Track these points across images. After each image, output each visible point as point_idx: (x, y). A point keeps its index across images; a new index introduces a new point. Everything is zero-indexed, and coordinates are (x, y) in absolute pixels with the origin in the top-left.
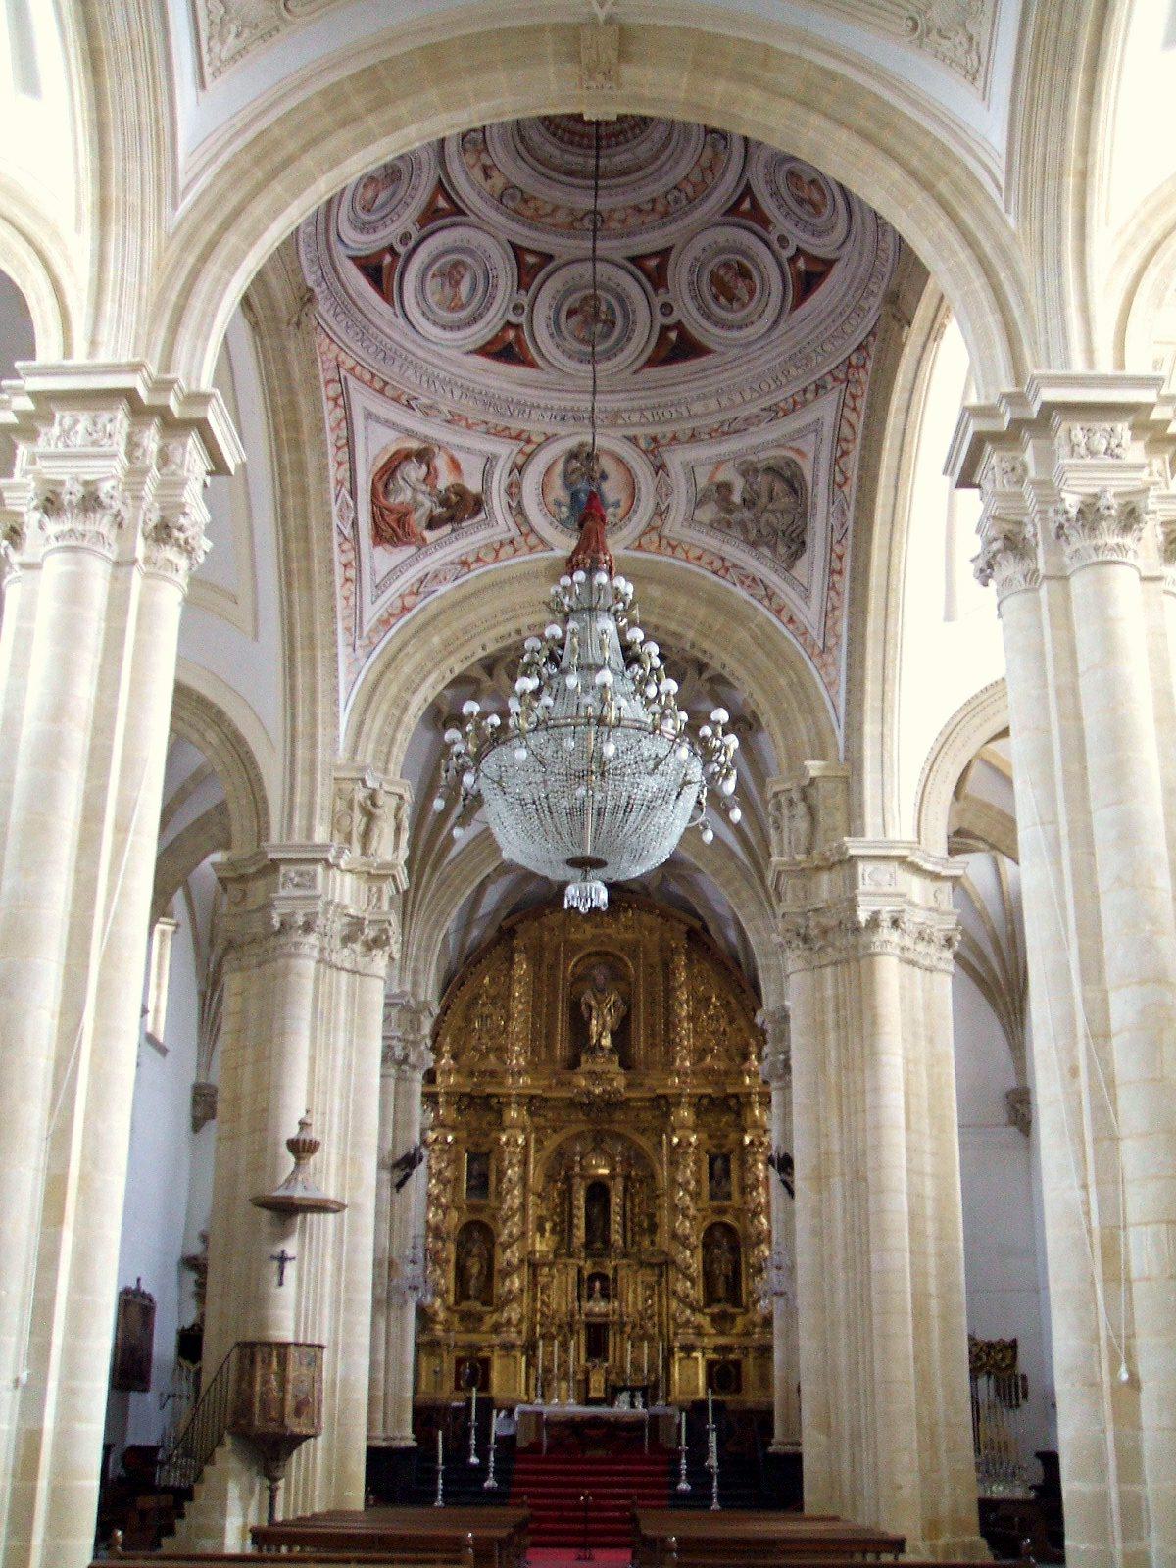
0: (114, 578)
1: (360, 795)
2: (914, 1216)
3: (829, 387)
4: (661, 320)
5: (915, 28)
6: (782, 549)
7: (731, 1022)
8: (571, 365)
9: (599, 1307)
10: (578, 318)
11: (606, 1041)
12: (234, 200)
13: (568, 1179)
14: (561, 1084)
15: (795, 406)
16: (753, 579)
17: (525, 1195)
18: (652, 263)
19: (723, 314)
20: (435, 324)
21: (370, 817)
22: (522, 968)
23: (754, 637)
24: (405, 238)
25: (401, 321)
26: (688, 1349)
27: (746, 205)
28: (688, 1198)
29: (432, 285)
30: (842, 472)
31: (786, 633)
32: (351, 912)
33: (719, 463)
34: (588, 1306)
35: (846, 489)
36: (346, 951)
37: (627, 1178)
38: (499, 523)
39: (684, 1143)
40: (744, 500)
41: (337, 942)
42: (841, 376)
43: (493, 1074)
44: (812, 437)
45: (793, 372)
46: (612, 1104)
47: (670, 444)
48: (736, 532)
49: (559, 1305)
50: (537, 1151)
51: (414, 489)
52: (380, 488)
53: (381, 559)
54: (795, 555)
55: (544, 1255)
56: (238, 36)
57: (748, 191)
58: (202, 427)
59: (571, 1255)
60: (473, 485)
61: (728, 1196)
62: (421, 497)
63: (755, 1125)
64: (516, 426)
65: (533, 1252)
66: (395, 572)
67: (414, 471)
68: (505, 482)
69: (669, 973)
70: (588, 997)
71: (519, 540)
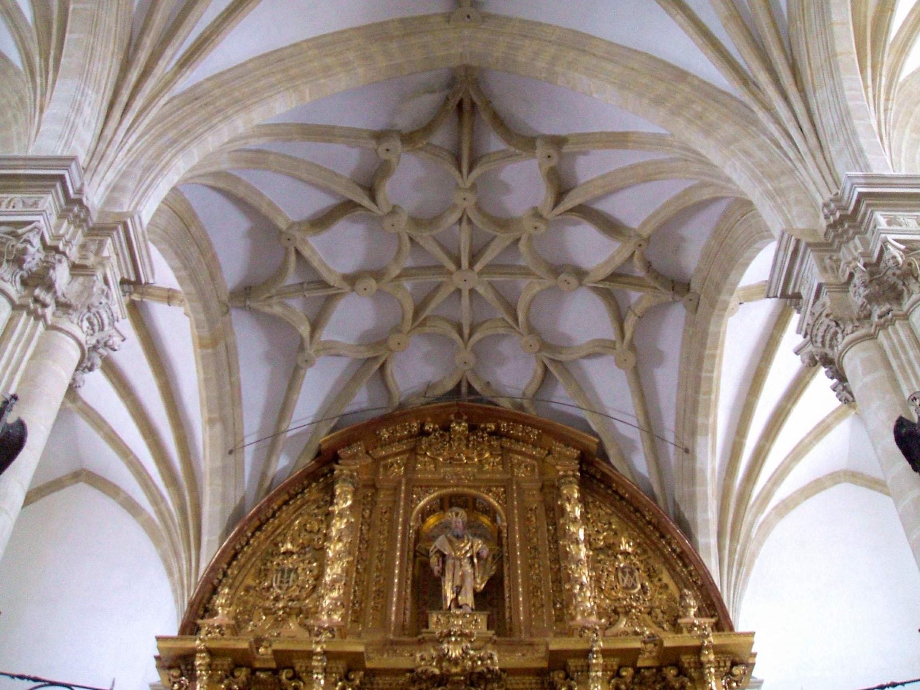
7: (651, 574)
11: (467, 599)
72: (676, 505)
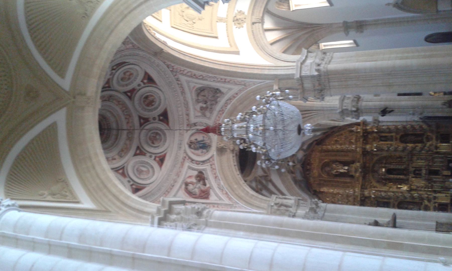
0: (211, 226)
1: (276, 207)
2: (402, 58)
3: (178, 77)
4: (157, 121)
5: (84, 17)
6: (218, 95)
7: (342, 135)
8: (167, 144)
9: (424, 172)
10: (155, 142)
11: (346, 168)
12: (111, 197)
13: (386, 179)
14: (358, 180)
15: (182, 87)
16: (226, 103)
17: (390, 192)
18: (142, 121)
19: (157, 103)
20: (152, 177)
21: (282, 205)
22: (324, 189)
23: (241, 104)
24: (129, 182)
25: (151, 185)
26: (437, 148)
27: (129, 94)
28: (392, 147)
29: (142, 177)
30: (200, 76)
31: (240, 95)
32: (308, 210)
33: (195, 109)
34: (423, 175)
35: (204, 76)
36: (319, 213)
37: (385, 164)
38: (206, 167)
39: (376, 147)
40: (205, 104)
41: (316, 215)
42: (175, 73)
43: (354, 199)
44: (190, 84)
45: (173, 87)
46: (364, 167)
47: (189, 121)
48: (213, 107)
49: (422, 183)
50: (377, 188)
51: (195, 188)
52: (194, 196)
53: (213, 198)
54: (220, 91)
55: (408, 188)
56: (66, 192)
57: (125, 93)
58: (171, 203)
59: (408, 180)
60: (196, 173)
61: (392, 136)
62: (197, 186)
63: (371, 128)
64: (181, 159)
65: (407, 191)
66: (217, 195)
67: (191, 187)
68: (196, 165)
69: (328, 151)
70: (334, 172)
71: (211, 163)
72: (328, 128)
